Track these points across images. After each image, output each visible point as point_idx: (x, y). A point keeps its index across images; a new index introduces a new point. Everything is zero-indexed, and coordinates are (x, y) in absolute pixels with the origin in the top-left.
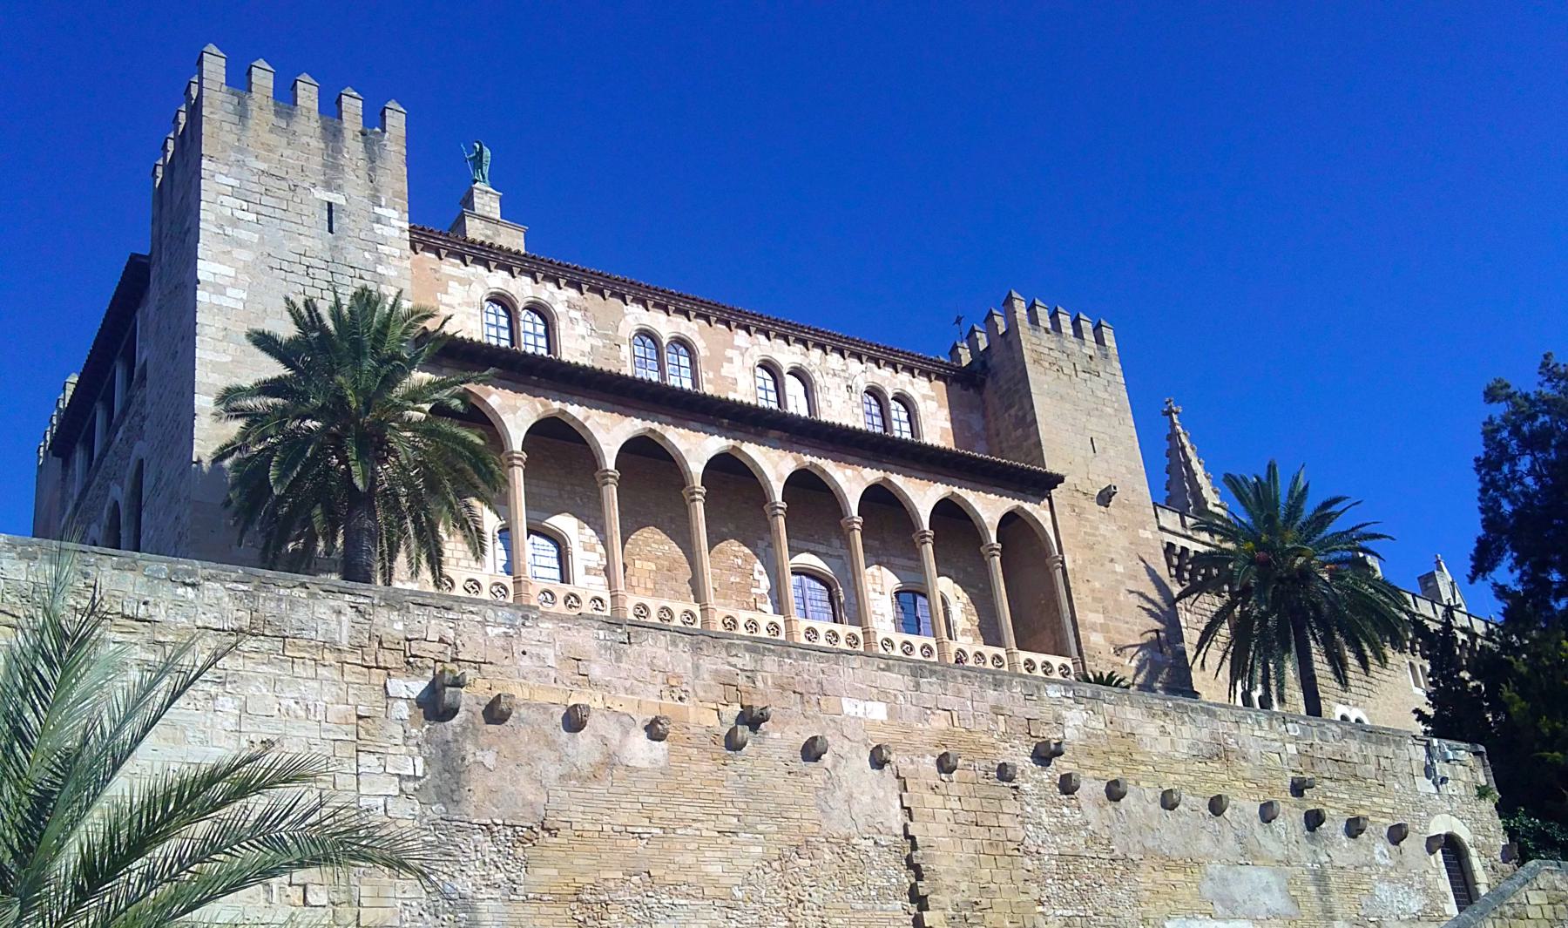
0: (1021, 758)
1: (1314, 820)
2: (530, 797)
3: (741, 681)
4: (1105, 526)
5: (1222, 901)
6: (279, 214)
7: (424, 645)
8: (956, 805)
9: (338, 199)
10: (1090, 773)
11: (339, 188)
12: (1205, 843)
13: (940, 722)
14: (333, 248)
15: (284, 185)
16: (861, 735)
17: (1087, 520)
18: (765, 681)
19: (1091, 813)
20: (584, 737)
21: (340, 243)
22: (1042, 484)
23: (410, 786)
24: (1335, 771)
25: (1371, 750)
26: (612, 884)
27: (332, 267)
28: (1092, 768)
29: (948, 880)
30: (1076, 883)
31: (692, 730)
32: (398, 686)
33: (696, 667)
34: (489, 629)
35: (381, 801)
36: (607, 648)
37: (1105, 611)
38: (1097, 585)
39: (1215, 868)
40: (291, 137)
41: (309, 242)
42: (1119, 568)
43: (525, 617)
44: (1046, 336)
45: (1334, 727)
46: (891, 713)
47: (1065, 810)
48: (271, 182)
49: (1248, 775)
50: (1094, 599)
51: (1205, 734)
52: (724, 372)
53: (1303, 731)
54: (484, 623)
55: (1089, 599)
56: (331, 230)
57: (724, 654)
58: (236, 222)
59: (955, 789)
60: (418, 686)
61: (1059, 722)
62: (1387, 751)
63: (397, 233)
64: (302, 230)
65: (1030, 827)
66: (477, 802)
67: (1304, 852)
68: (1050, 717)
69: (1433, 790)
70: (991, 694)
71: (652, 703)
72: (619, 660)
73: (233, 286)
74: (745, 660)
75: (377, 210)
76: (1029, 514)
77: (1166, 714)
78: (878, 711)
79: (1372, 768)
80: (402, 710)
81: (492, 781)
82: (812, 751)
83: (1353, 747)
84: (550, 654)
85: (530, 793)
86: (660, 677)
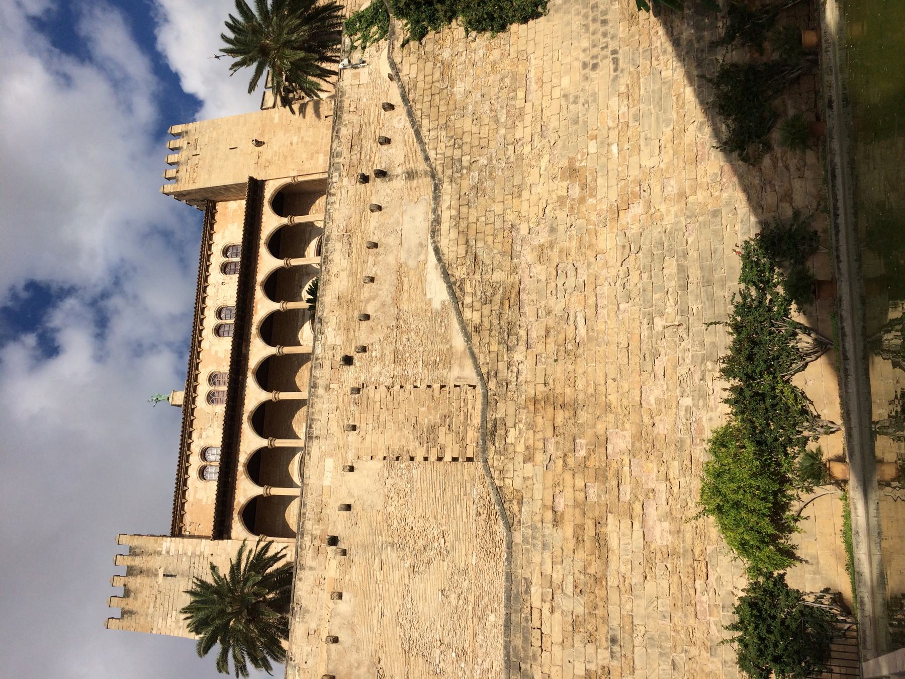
0: (351, 376)
1: (381, 174)
2: (366, 669)
3: (317, 543)
5: (419, 255)
6: (171, 600)
8: (370, 427)
9: (161, 572)
10: (357, 334)
11: (156, 570)
12: (391, 259)
13: (334, 427)
15: (158, 596)
18: (316, 529)
19: (375, 337)
22: (255, 187)
24: (356, 148)
25: (346, 117)
26: (402, 634)
30: (407, 355)
31: (338, 577)
33: (311, 568)
36: (303, 618)
37: (317, 152)
38: (304, 156)
39: (403, 257)
43: (291, 659)
44: (180, 173)
46: (331, 456)
47: (374, 354)
48: (157, 605)
49: (358, 218)
51: (338, 246)
52: (222, 356)
53: (336, 170)
55: (312, 162)
56: (175, 576)
57: (304, 552)
59: (363, 425)
61: (334, 347)
62: (346, 104)
63: (173, 544)
65: (381, 379)
67: (398, 183)
68: (331, 353)
69: (366, 70)
70: (321, 391)
71: (326, 596)
72: (307, 611)
74: (307, 538)
75: (164, 552)
76: (272, 196)
78: (329, 463)
79: (354, 118)
82: (348, 507)
83: (344, 131)
84: (307, 649)
85: (363, 670)
86: (316, 589)
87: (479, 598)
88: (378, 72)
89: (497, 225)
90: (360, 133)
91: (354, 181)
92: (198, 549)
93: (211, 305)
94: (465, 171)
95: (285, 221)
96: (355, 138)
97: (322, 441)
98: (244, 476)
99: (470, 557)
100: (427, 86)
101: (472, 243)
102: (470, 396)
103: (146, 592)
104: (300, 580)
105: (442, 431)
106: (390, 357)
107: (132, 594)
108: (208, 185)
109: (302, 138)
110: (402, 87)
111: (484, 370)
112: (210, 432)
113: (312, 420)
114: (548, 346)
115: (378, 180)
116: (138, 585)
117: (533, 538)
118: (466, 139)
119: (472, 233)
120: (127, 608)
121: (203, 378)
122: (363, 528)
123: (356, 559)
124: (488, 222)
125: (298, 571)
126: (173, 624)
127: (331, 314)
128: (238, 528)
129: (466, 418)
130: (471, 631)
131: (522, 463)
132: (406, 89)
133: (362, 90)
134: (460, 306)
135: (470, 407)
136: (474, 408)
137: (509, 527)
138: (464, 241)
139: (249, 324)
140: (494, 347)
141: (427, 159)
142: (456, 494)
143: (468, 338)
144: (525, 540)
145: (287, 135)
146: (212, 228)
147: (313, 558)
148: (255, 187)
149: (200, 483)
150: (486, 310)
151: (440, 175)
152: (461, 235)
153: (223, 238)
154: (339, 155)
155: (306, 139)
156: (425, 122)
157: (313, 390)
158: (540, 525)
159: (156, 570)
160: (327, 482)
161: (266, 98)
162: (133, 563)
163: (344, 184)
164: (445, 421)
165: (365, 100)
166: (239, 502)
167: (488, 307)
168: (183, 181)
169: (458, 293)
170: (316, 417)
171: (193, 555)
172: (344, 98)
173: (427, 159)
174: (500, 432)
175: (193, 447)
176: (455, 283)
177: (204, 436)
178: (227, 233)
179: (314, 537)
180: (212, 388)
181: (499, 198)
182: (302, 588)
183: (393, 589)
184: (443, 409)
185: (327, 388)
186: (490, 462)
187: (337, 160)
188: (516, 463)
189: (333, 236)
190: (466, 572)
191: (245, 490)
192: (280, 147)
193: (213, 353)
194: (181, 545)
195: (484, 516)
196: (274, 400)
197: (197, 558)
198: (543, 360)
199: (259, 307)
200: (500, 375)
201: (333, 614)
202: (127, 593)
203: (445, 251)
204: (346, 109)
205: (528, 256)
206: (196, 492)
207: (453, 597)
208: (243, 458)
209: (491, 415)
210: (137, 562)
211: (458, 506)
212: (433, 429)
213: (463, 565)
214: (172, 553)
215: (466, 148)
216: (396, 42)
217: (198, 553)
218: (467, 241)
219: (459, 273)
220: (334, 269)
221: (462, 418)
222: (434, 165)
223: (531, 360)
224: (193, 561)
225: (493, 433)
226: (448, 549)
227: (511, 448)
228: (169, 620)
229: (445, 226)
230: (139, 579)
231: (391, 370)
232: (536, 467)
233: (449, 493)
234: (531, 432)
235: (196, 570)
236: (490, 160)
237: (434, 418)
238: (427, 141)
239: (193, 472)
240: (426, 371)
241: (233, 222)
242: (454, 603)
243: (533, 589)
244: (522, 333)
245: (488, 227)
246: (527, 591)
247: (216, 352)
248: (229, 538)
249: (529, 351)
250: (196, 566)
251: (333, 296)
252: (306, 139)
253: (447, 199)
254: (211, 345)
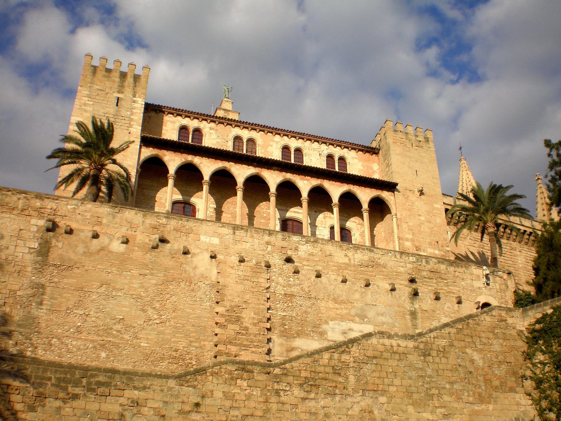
0: (277, 260)
4: (420, 204)
6: (101, 101)
7: (46, 210)
8: (241, 273)
11: (122, 93)
14: (118, 111)
15: (104, 93)
16: (206, 247)
17: (410, 200)
20: (95, 241)
21: (120, 109)
23: (32, 250)
25: (452, 269)
27: (115, 117)
28: (307, 266)
29: (229, 298)
30: (290, 304)
32: (34, 221)
33: (143, 222)
34: (68, 206)
35: (22, 254)
38: (411, 224)
40: (108, 77)
41: (107, 109)
42: (422, 218)
43: (82, 203)
45: (433, 259)
46: (221, 242)
47: (291, 279)
50: (409, 229)
51: (366, 258)
53: (418, 260)
54: (67, 205)
55: (407, 229)
56: (117, 105)
57: (155, 218)
58: (85, 105)
60: (42, 223)
61: (296, 249)
62: (460, 270)
63: (140, 106)
64: (107, 106)
66: (54, 257)
69: (482, 286)
70: (267, 238)
71: (124, 231)
74: (164, 221)
75: (134, 99)
77: (349, 250)
78: (216, 241)
80: (34, 229)
81: (60, 252)
83: (443, 267)
84: (88, 215)
85: (73, 256)
86: (129, 225)
87: (117, 346)
88: (481, 294)
89: (386, 380)
90: (442, 279)
91: (409, 272)
92: (135, 123)
93: (306, 146)
94: (422, 358)
95: (365, 206)
96: (438, 275)
97: (232, 237)
98: (184, 160)
99: (146, 342)
100: (477, 333)
101: (375, 361)
102: (260, 350)
103: (108, 84)
104: (136, 214)
105: (236, 327)
106: (289, 291)
107: (107, 74)
108: (392, 152)
109: (423, 224)
110: (477, 316)
111: (288, 366)
112: (214, 136)
113: (247, 231)
114: (304, 414)
115: (410, 289)
116: (113, 78)
117: (172, 395)
118: (444, 360)
119: (381, 361)
120: (98, 70)
121: (253, 134)
122: (170, 263)
123: (148, 256)
124: (389, 374)
125: (142, 213)
126: (83, 102)
127: (319, 249)
128: (148, 152)
129: (245, 346)
130: (95, 338)
131: (222, 390)
132: (476, 318)
133: (469, 281)
134: (332, 350)
135: (253, 349)
136: (253, 352)
137: (179, 377)
138: (376, 355)
139: (293, 173)
140: (304, 374)
141: (431, 331)
142: (191, 335)
143: (310, 354)
144: (170, 389)
145: (425, 213)
146: (360, 150)
147: (151, 224)
148: (391, 187)
149: (177, 126)
150: (329, 370)
151: (420, 340)
152: (379, 353)
153: (353, 158)
154: (427, 262)
155: (423, 226)
156: (453, 331)
157: (268, 232)
158: (180, 400)
160: (202, 238)
161: (449, 198)
162: (129, 76)
163: (408, 265)
164: (243, 330)
165: (463, 283)
166: (165, 155)
167: (331, 371)
168: (394, 135)
169: (341, 349)
170: (249, 234)
171: (131, 120)
172: (464, 269)
173: (431, 331)
174: (245, 375)
175: (204, 122)
176: (347, 347)
177: (212, 131)
178: (356, 161)
179: (164, 226)
180: (245, 141)
181: (404, 382)
182: (131, 215)
183: (126, 282)
184: (253, 330)
185: (268, 243)
186: (224, 366)
187: (424, 260)
188: (223, 386)
189: (372, 254)
190: (136, 337)
191: (174, 160)
192: (417, 207)
193: (271, 143)
194: (139, 111)
195: (174, 354)
196: (237, 187)
197: (128, 122)
198: (294, 410)
199: (305, 182)
200: (284, 378)
201: (111, 238)
202: (109, 71)
203: (369, 342)
204: (457, 269)
205: (366, 402)
206: (172, 122)
207: (118, 327)
208: (197, 160)
209: (257, 369)
210: (130, 80)
211: (182, 336)
212: (238, 320)
213: (141, 336)
214: (136, 105)
215: (437, 360)
216: (504, 312)
217: (132, 123)
218: (376, 358)
219: (355, 350)
220: (350, 254)
221: (245, 343)
222: (427, 336)
223: (294, 401)
225: (243, 369)
226: (153, 326)
227: (233, 383)
228: (87, 99)
229: (387, 342)
230: (118, 80)
231: (280, 290)
232: (219, 401)
233: (192, 329)
234: (244, 398)
235: (120, 121)
236: (430, 377)
237: (247, 323)
238: (442, 332)
239: (186, 121)
240: (278, 317)
241: (363, 166)
242: (115, 327)
243: (136, 392)
244: (312, 395)
245: (385, 374)
246: (135, 388)
247: (272, 146)
248: (141, 147)
249: (300, 399)
251: (332, 252)
252: (423, 226)
253: (403, 343)
254: (277, 143)
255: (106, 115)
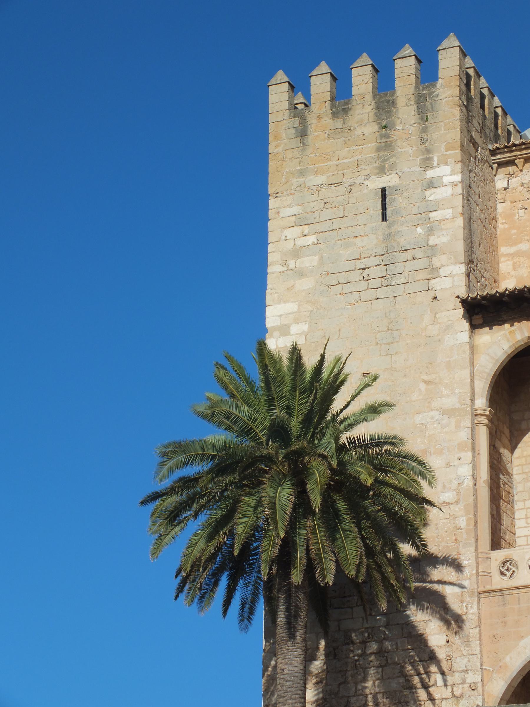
6: (336, 224)
9: (388, 180)
15: (341, 189)
21: (394, 229)
58: (297, 253)
73: (297, 321)
75: (430, 174)
92: (444, 259)
107: (339, 124)
120: (312, 120)
126: (290, 245)
159: (393, 166)
162: (401, 102)
171: (432, 251)
194: (448, 213)
210: (405, 112)
217: (436, 262)
224: (419, 254)
228: (297, 230)
230: (371, 129)
235: (400, 267)
250: (411, 265)
255: (360, 264)
